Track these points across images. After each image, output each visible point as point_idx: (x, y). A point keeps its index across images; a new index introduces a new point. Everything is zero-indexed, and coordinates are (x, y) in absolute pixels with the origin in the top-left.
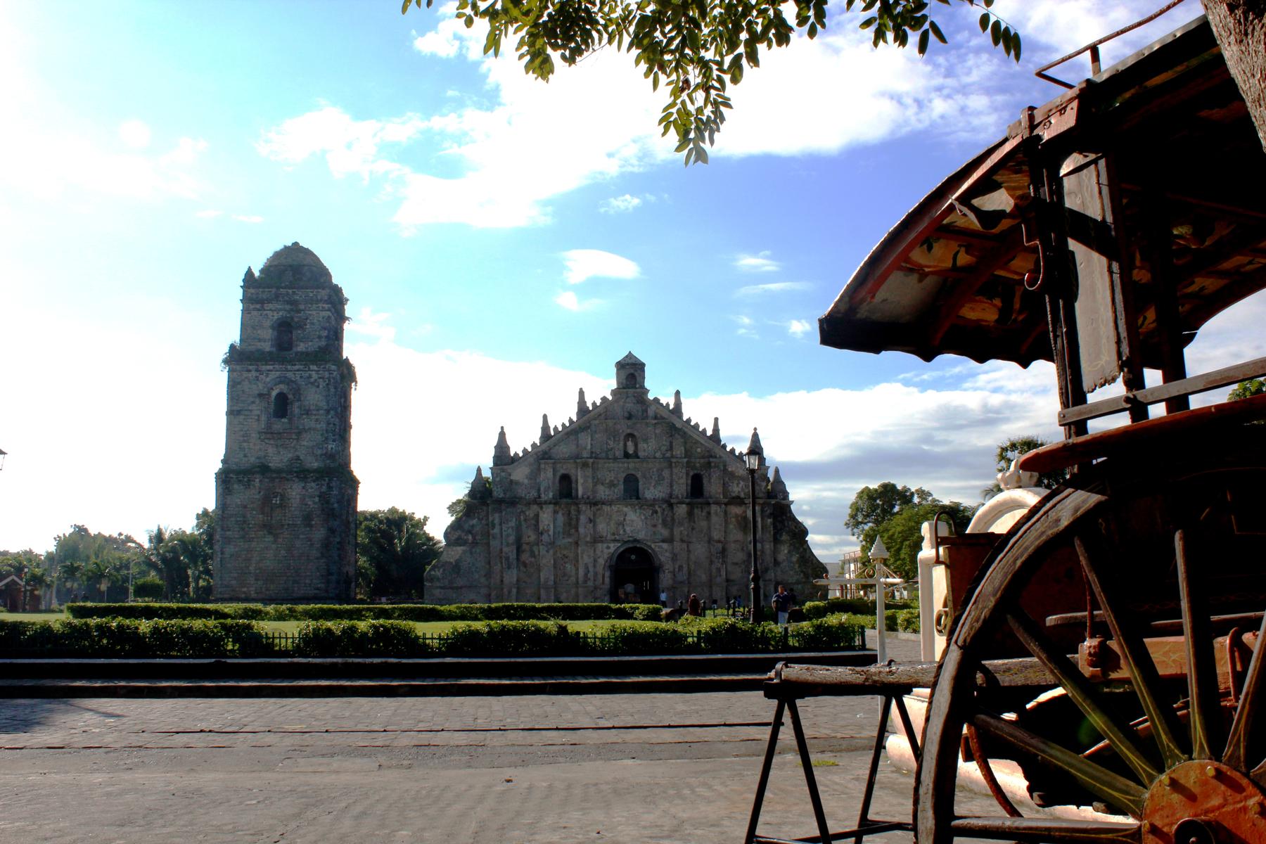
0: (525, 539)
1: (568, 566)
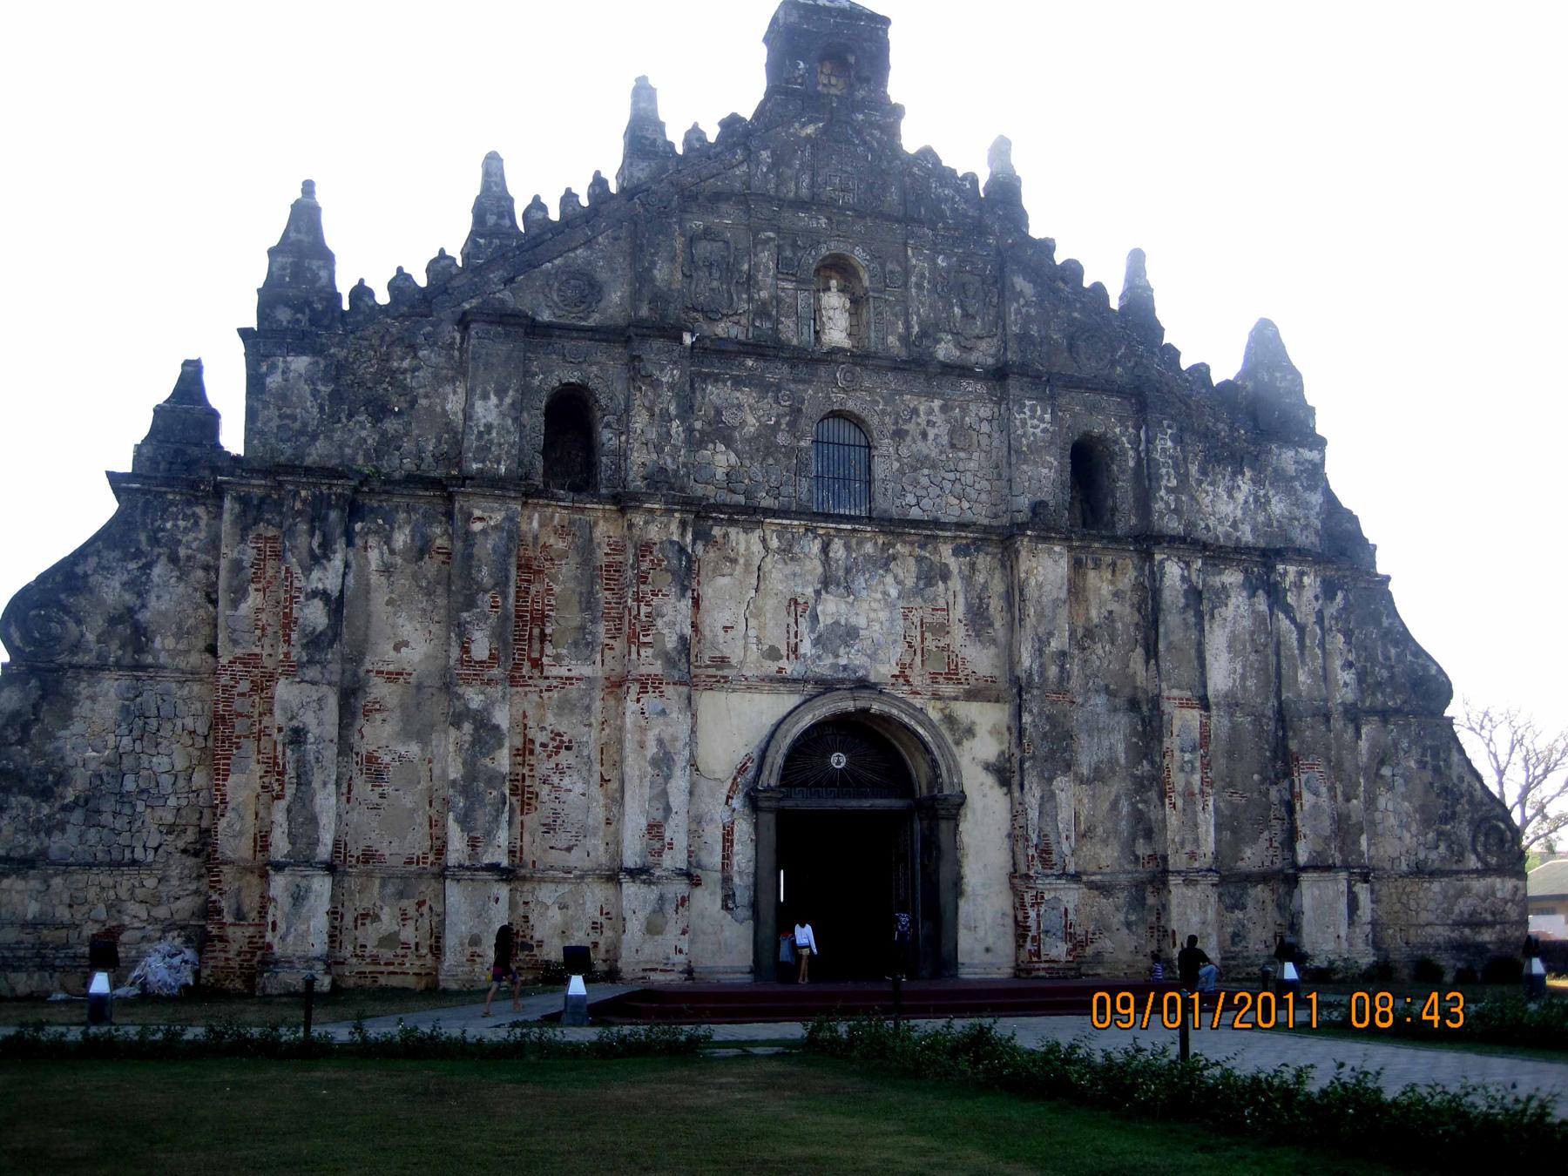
0: (383, 655)
1: (574, 785)
